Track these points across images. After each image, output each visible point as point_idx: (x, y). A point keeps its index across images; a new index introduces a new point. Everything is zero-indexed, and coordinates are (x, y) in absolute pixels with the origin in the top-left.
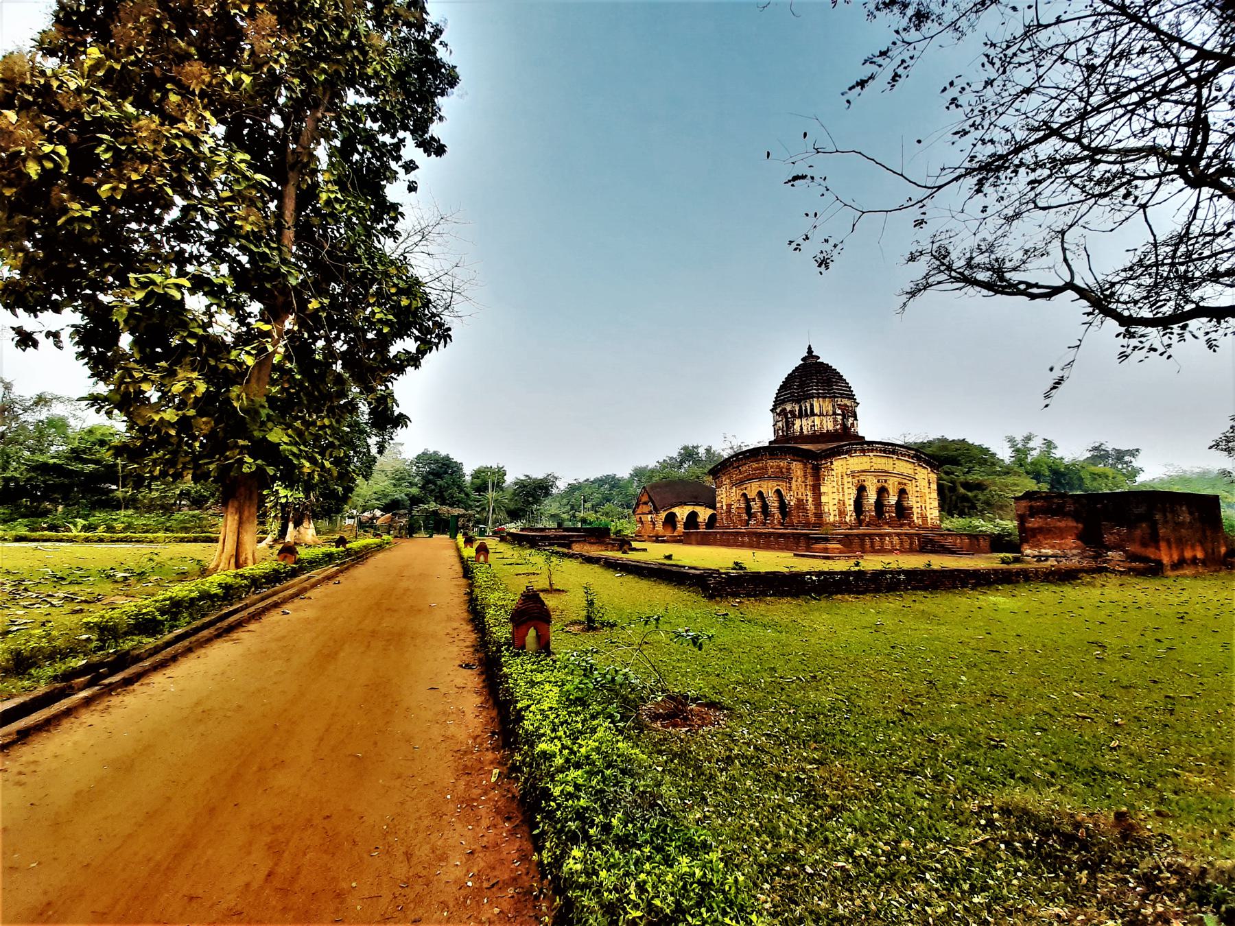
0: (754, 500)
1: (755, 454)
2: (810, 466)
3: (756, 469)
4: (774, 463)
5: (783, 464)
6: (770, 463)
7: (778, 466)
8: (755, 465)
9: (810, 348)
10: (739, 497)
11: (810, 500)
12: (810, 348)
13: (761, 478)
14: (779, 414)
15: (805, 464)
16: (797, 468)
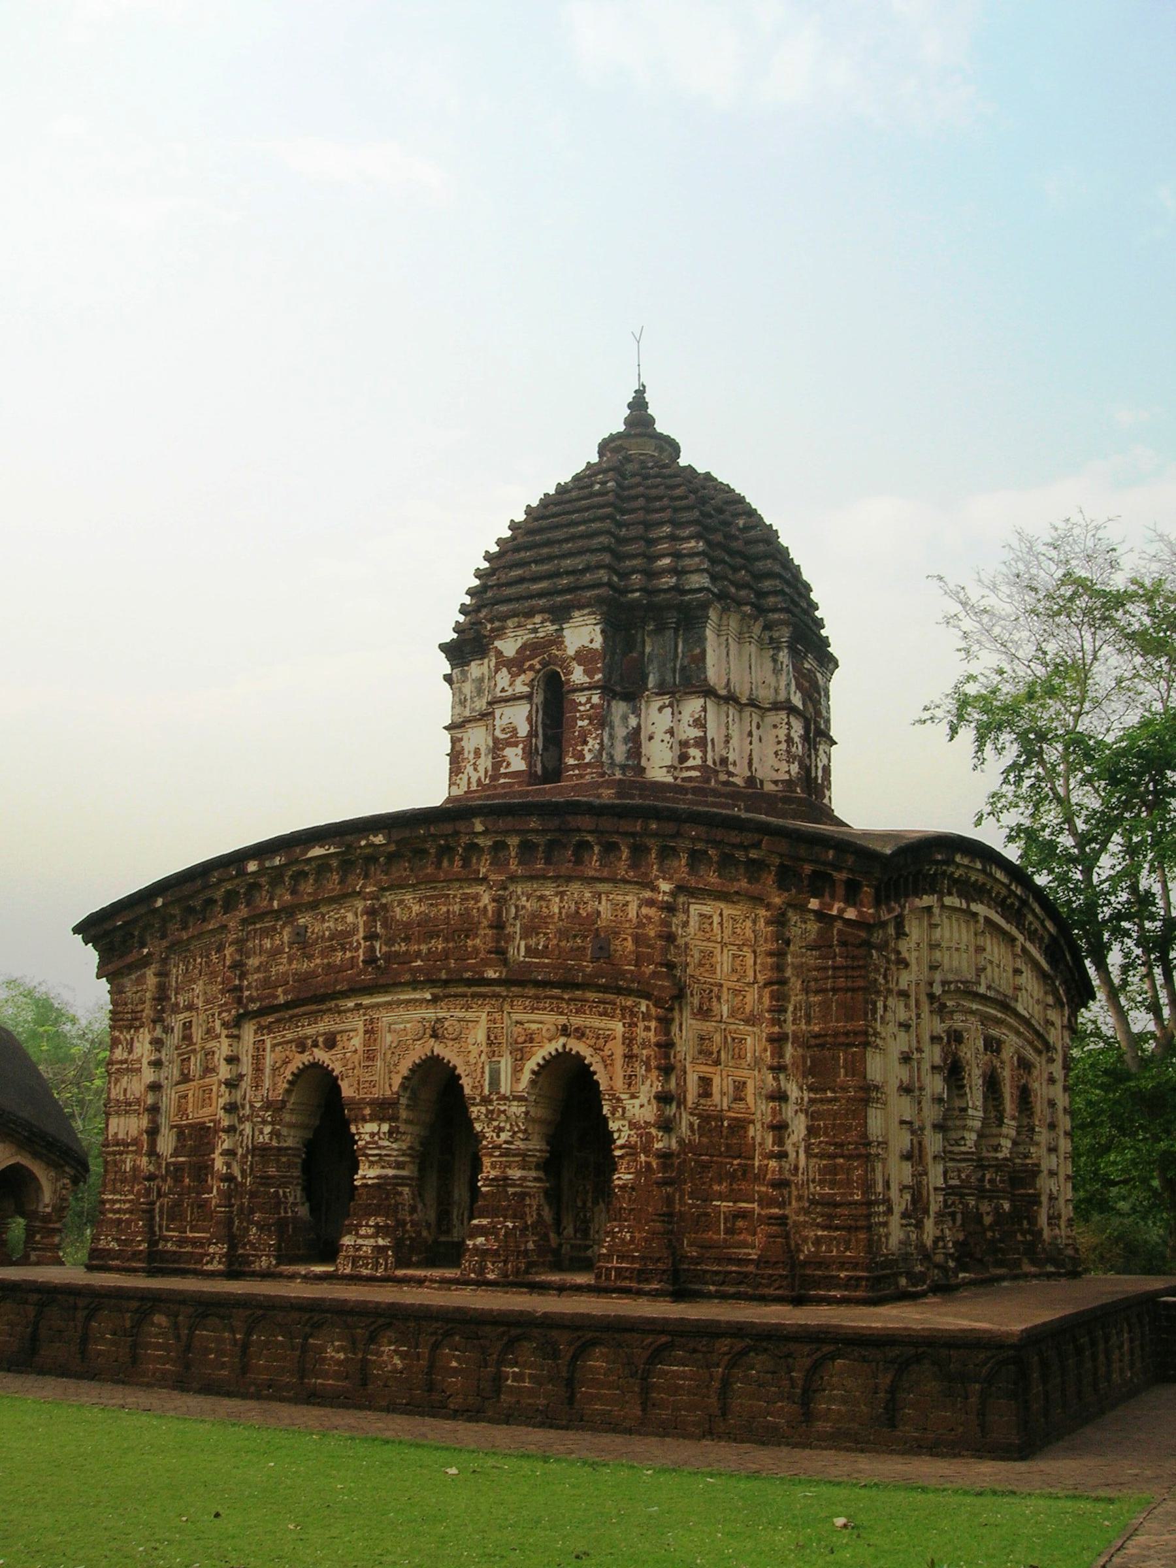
0: (383, 1109)
1: (407, 841)
2: (804, 929)
3: (427, 928)
4: (559, 902)
6: (524, 898)
7: (582, 924)
8: (409, 906)
9: (639, 404)
10: (275, 1086)
11: (799, 1127)
12: (639, 404)
13: (452, 982)
14: (516, 665)
15: (779, 921)
16: (724, 937)
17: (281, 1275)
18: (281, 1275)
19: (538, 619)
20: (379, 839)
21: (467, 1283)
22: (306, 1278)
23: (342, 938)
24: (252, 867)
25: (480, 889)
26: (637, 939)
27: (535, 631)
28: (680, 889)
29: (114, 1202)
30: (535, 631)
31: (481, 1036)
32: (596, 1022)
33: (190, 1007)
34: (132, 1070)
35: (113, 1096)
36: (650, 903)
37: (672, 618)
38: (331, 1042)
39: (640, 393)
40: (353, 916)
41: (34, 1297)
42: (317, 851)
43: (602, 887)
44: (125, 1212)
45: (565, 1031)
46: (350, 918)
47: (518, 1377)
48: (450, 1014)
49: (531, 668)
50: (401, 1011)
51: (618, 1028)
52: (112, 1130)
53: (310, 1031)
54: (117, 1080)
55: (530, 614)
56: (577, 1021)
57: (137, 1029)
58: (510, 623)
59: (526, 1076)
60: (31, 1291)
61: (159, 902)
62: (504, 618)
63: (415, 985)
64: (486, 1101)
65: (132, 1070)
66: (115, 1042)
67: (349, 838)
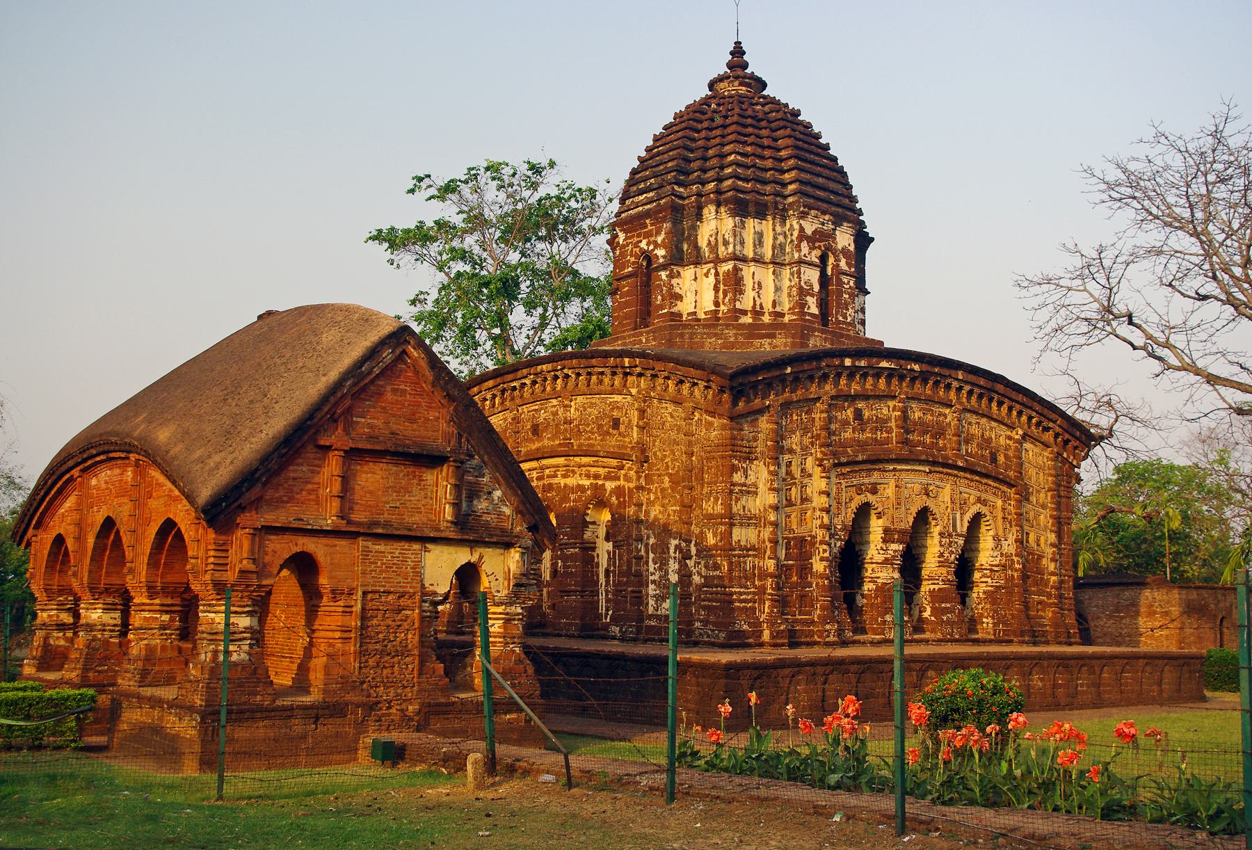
5: (1001, 436)
9: (738, 51)
12: (738, 51)
17: (854, 642)
18: (859, 642)
19: (827, 217)
20: (917, 367)
21: (948, 641)
22: (872, 643)
23: (882, 423)
24: (848, 362)
25: (947, 411)
26: (1006, 456)
27: (823, 224)
28: (1025, 436)
29: (741, 594)
30: (823, 224)
31: (947, 499)
32: (991, 498)
33: (791, 451)
34: (749, 492)
35: (735, 510)
36: (1010, 438)
37: (751, 209)
38: (874, 491)
39: (738, 43)
40: (890, 410)
41: (854, 668)
42: (884, 364)
43: (994, 424)
44: (750, 601)
45: (979, 500)
46: (885, 411)
47: (1082, 685)
48: (933, 480)
49: (819, 247)
50: (912, 476)
51: (999, 503)
52: (735, 538)
53: (866, 481)
54: (737, 500)
55: (824, 213)
56: (984, 496)
57: (751, 461)
58: (813, 212)
59: (966, 524)
60: (853, 664)
61: (789, 370)
62: (811, 208)
63: (921, 462)
64: (950, 536)
65: (749, 492)
66: (734, 469)
67: (902, 362)
